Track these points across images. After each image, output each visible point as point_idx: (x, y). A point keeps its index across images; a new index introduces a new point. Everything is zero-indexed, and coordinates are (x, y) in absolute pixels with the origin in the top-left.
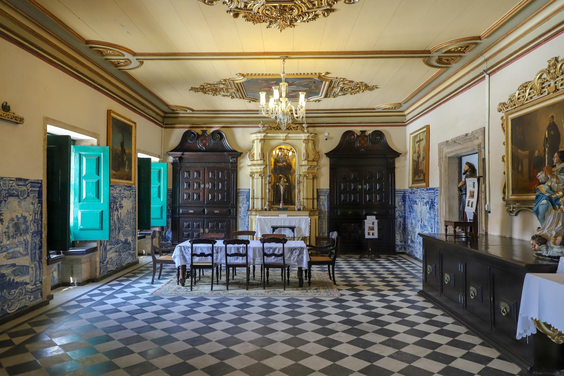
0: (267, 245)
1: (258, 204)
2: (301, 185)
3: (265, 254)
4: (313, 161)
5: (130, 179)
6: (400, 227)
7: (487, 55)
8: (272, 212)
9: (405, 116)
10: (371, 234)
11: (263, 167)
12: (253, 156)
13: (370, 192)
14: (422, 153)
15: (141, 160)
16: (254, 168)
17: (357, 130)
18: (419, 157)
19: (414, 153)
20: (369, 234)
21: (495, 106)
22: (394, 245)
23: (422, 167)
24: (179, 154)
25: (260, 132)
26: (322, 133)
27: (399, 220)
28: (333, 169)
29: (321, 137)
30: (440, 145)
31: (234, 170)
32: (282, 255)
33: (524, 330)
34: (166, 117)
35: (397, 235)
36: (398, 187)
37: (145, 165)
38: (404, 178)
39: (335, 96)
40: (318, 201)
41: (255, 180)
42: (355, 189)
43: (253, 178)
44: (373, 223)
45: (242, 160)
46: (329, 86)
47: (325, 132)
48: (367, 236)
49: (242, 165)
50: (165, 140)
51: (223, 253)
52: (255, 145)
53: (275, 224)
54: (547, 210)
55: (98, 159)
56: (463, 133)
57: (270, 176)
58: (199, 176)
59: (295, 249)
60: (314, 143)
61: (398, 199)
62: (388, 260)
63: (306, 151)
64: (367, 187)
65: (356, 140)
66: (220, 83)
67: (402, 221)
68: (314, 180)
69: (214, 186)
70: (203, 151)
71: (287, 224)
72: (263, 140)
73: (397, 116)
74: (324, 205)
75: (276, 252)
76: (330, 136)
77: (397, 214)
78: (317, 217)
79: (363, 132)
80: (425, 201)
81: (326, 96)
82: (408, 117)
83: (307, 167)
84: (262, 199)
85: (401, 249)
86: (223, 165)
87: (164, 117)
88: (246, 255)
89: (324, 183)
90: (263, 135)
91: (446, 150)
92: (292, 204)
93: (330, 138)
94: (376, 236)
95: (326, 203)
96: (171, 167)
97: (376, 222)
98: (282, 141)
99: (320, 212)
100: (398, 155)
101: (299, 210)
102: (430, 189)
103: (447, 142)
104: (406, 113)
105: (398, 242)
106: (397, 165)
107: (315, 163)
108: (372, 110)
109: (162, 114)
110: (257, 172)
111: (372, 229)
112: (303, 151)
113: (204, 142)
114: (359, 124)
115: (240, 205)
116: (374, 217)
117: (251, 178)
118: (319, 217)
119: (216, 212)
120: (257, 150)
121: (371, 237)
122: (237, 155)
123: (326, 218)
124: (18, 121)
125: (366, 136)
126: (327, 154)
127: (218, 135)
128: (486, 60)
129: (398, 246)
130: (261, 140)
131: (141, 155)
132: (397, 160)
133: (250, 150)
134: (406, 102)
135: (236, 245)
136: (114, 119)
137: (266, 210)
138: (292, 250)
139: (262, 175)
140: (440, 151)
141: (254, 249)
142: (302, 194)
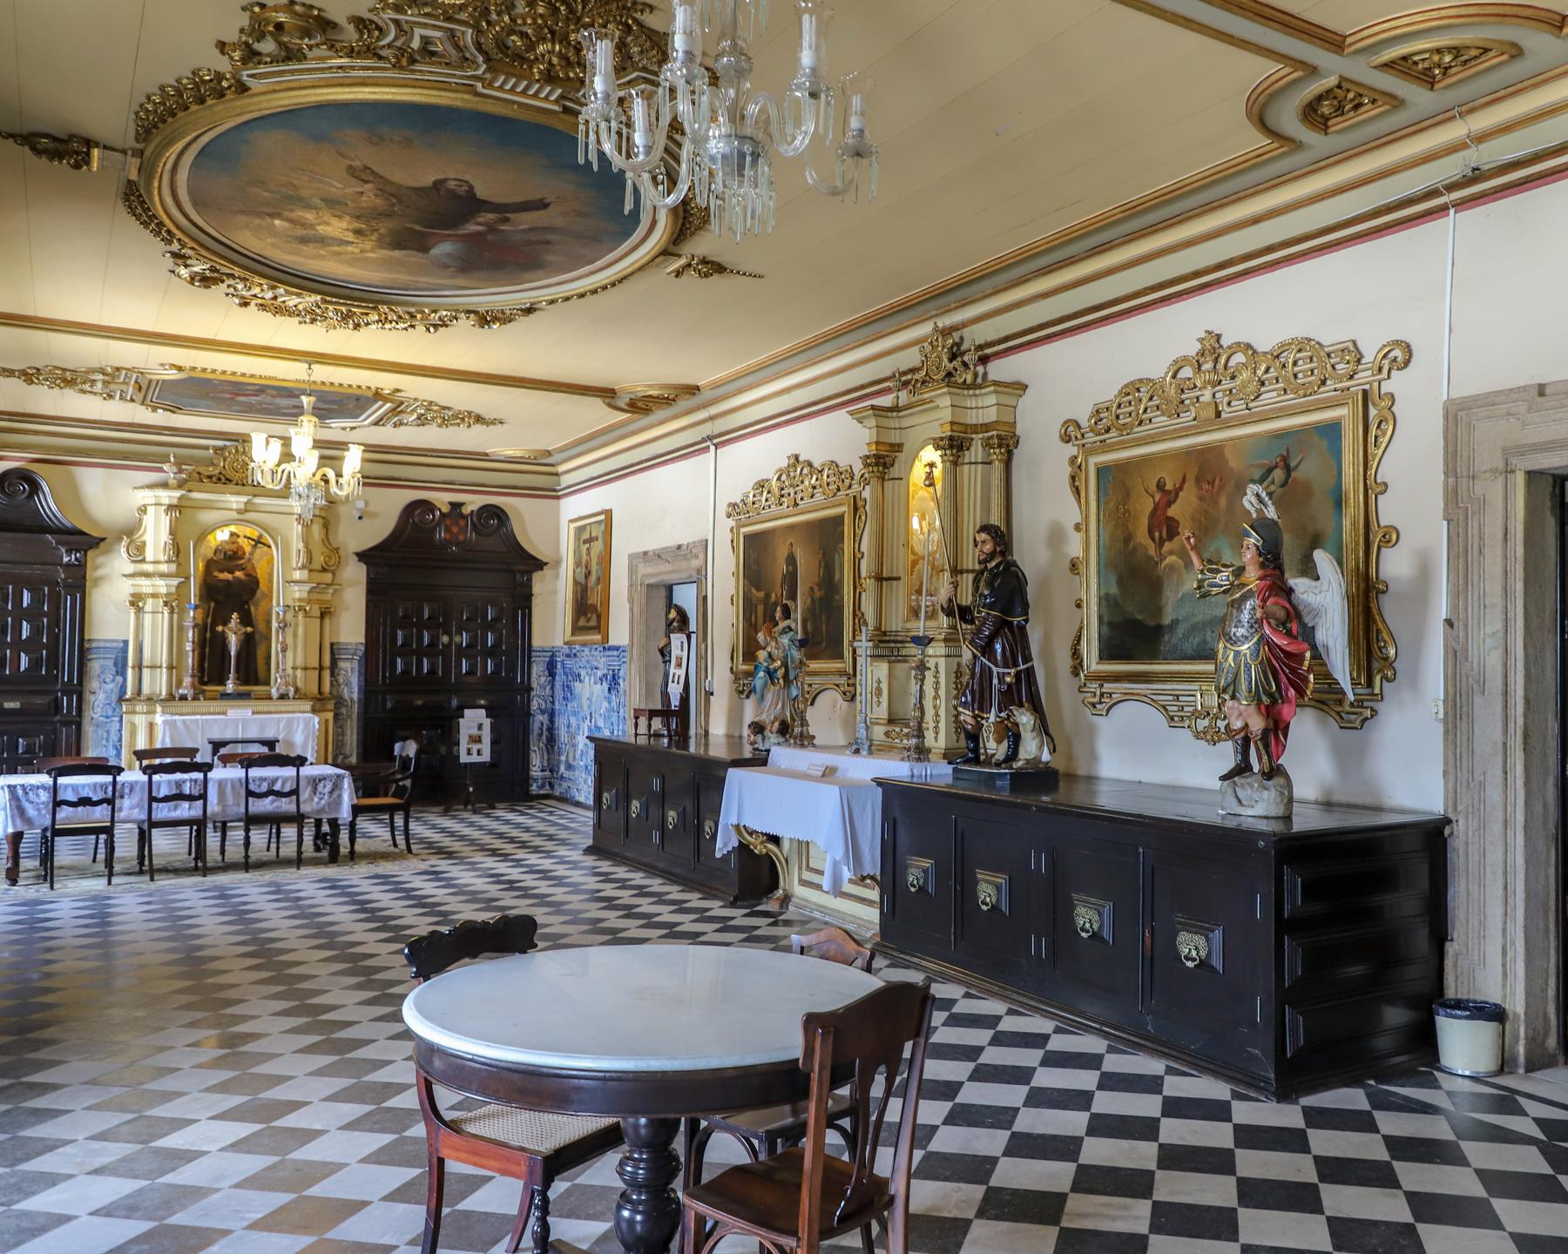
1: (156, 682)
2: (289, 631)
3: (250, 794)
4: (324, 570)
6: (541, 735)
7: (713, 410)
8: (202, 704)
9: (556, 474)
10: (475, 752)
11: (175, 582)
12: (141, 548)
13: (468, 651)
14: (594, 568)
16: (143, 581)
17: (442, 499)
19: (578, 564)
20: (469, 752)
21: (722, 509)
22: (526, 779)
23: (594, 599)
25: (164, 485)
27: (539, 719)
28: (376, 594)
30: (632, 557)
31: (78, 583)
32: (295, 792)
33: (724, 844)
35: (533, 755)
36: (537, 641)
38: (551, 623)
40: (332, 675)
41: (148, 618)
42: (434, 643)
43: (139, 610)
44: (480, 727)
45: (101, 560)
48: (464, 758)
49: (100, 572)
51: (140, 796)
52: (149, 520)
53: (217, 735)
56: (671, 542)
57: (196, 607)
59: (323, 779)
60: (326, 526)
61: (538, 670)
62: (514, 811)
63: (306, 546)
64: (464, 639)
65: (439, 524)
67: (546, 722)
68: (317, 619)
71: (253, 734)
74: (348, 684)
75: (277, 787)
76: (372, 508)
77: (534, 705)
78: (330, 716)
79: (456, 506)
80: (599, 674)
82: (566, 480)
83: (307, 587)
84: (170, 668)
85: (542, 787)
86: (37, 570)
88: (203, 796)
89: (351, 628)
90: (178, 494)
91: (644, 570)
92: (257, 683)
94: (486, 757)
95: (355, 681)
97: (487, 722)
98: (234, 515)
99: (339, 702)
100: (539, 565)
101: (283, 697)
102: (610, 648)
103: (645, 553)
104: (561, 469)
105: (535, 772)
107: (328, 577)
108: (484, 456)
110: (154, 596)
111: (478, 740)
112: (297, 544)
114: (448, 485)
115: (94, 684)
116: (483, 711)
117: (133, 606)
118: (336, 717)
119: (9, 705)
120: (156, 533)
121: (475, 758)
123: (355, 716)
125: (464, 517)
126: (363, 556)
128: (712, 418)
129: (535, 780)
130: (170, 507)
132: (537, 577)
133: (130, 531)
134: (561, 450)
135: (178, 776)
137: (183, 698)
138: (315, 782)
139: (174, 603)
140: (632, 570)
141: (221, 784)
142: (290, 655)
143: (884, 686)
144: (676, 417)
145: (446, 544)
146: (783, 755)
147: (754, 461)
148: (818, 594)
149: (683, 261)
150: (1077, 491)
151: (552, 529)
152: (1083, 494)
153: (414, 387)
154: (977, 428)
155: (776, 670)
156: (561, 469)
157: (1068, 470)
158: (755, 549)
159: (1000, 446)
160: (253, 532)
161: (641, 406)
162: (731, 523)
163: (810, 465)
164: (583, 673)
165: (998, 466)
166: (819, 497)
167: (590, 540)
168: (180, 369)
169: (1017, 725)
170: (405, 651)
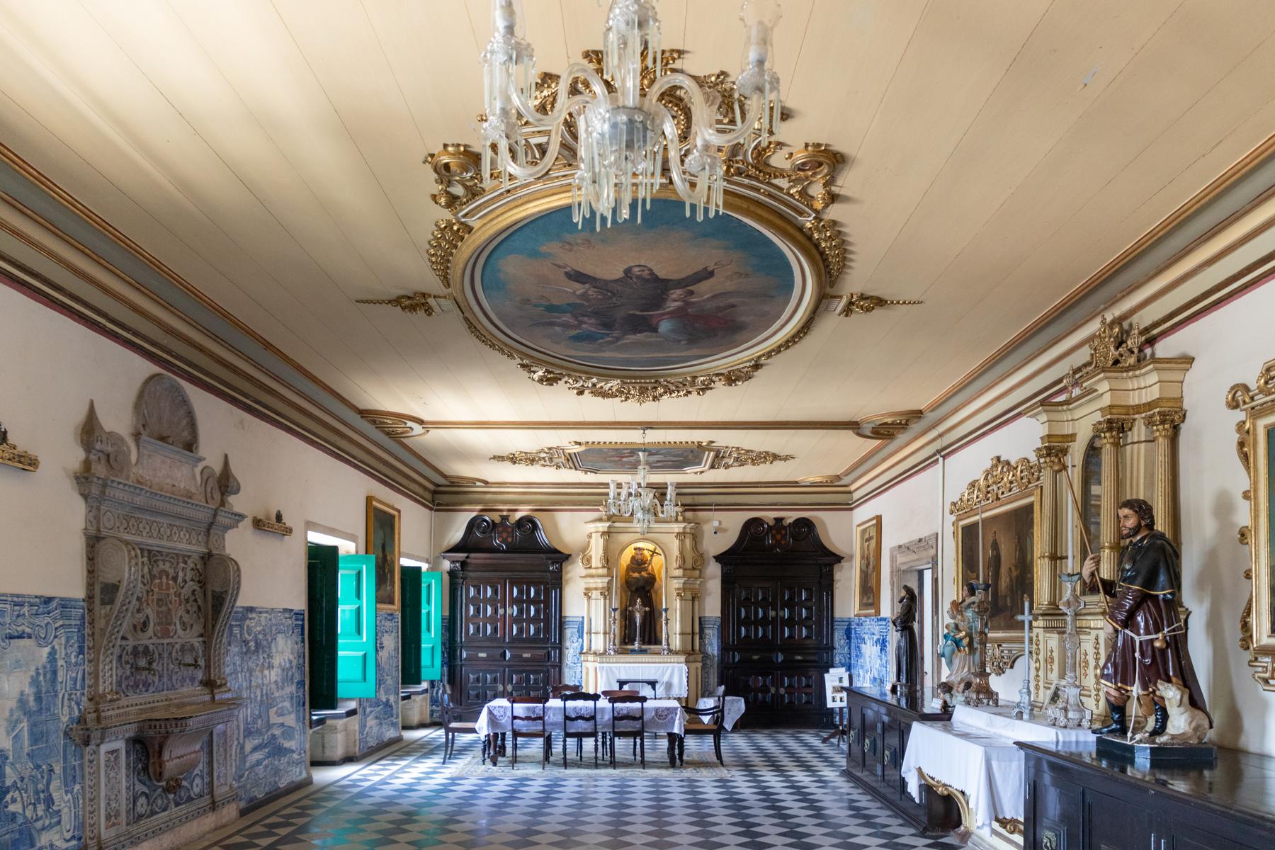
0: (618, 705)
4: (694, 569)
5: (392, 602)
9: (850, 492)
11: (606, 580)
12: (589, 560)
14: (871, 559)
15: (405, 570)
16: (591, 580)
17: (769, 516)
18: (868, 564)
19: (862, 557)
24: (462, 556)
25: (600, 520)
26: (708, 521)
29: (708, 529)
31: (556, 582)
34: (442, 493)
37: (412, 578)
38: (847, 602)
39: (727, 467)
41: (593, 602)
43: (589, 598)
45: (570, 568)
46: (717, 456)
47: (714, 520)
49: (569, 575)
50: (437, 533)
52: (593, 541)
54: (953, 652)
55: (359, 574)
58: (496, 593)
63: (681, 553)
65: (767, 534)
66: (542, 451)
69: (520, 611)
70: (503, 552)
72: (607, 534)
73: (838, 495)
76: (723, 526)
81: (712, 467)
82: (856, 496)
87: (434, 493)
89: (712, 607)
91: (901, 559)
93: (723, 530)
96: (447, 577)
98: (639, 536)
103: (900, 547)
104: (852, 488)
106: (837, 576)
108: (795, 484)
109: (431, 487)
113: (505, 535)
120: (596, 550)
122: (560, 558)
124: (289, 531)
125: (785, 528)
126: (718, 558)
127: (529, 525)
130: (603, 533)
131: (406, 562)
132: (836, 567)
133: (584, 549)
134: (847, 473)
136: (376, 509)
139: (606, 592)
140: (893, 559)
142: (673, 628)
143: (1056, 654)
144: (916, 438)
145: (772, 547)
146: (964, 715)
147: (970, 465)
148: (1014, 574)
149: (844, 301)
150: (1245, 457)
151: (840, 531)
152: (1251, 460)
153: (724, 439)
154: (1138, 409)
155: (961, 639)
156: (852, 488)
157: (1236, 437)
158: (969, 534)
159: (1163, 422)
160: (651, 547)
161: (885, 431)
162: (953, 518)
163: (1008, 463)
164: (866, 637)
165: (1162, 443)
166: (1015, 490)
167: (869, 539)
168: (579, 444)
169: (1163, 698)
170: (747, 622)
